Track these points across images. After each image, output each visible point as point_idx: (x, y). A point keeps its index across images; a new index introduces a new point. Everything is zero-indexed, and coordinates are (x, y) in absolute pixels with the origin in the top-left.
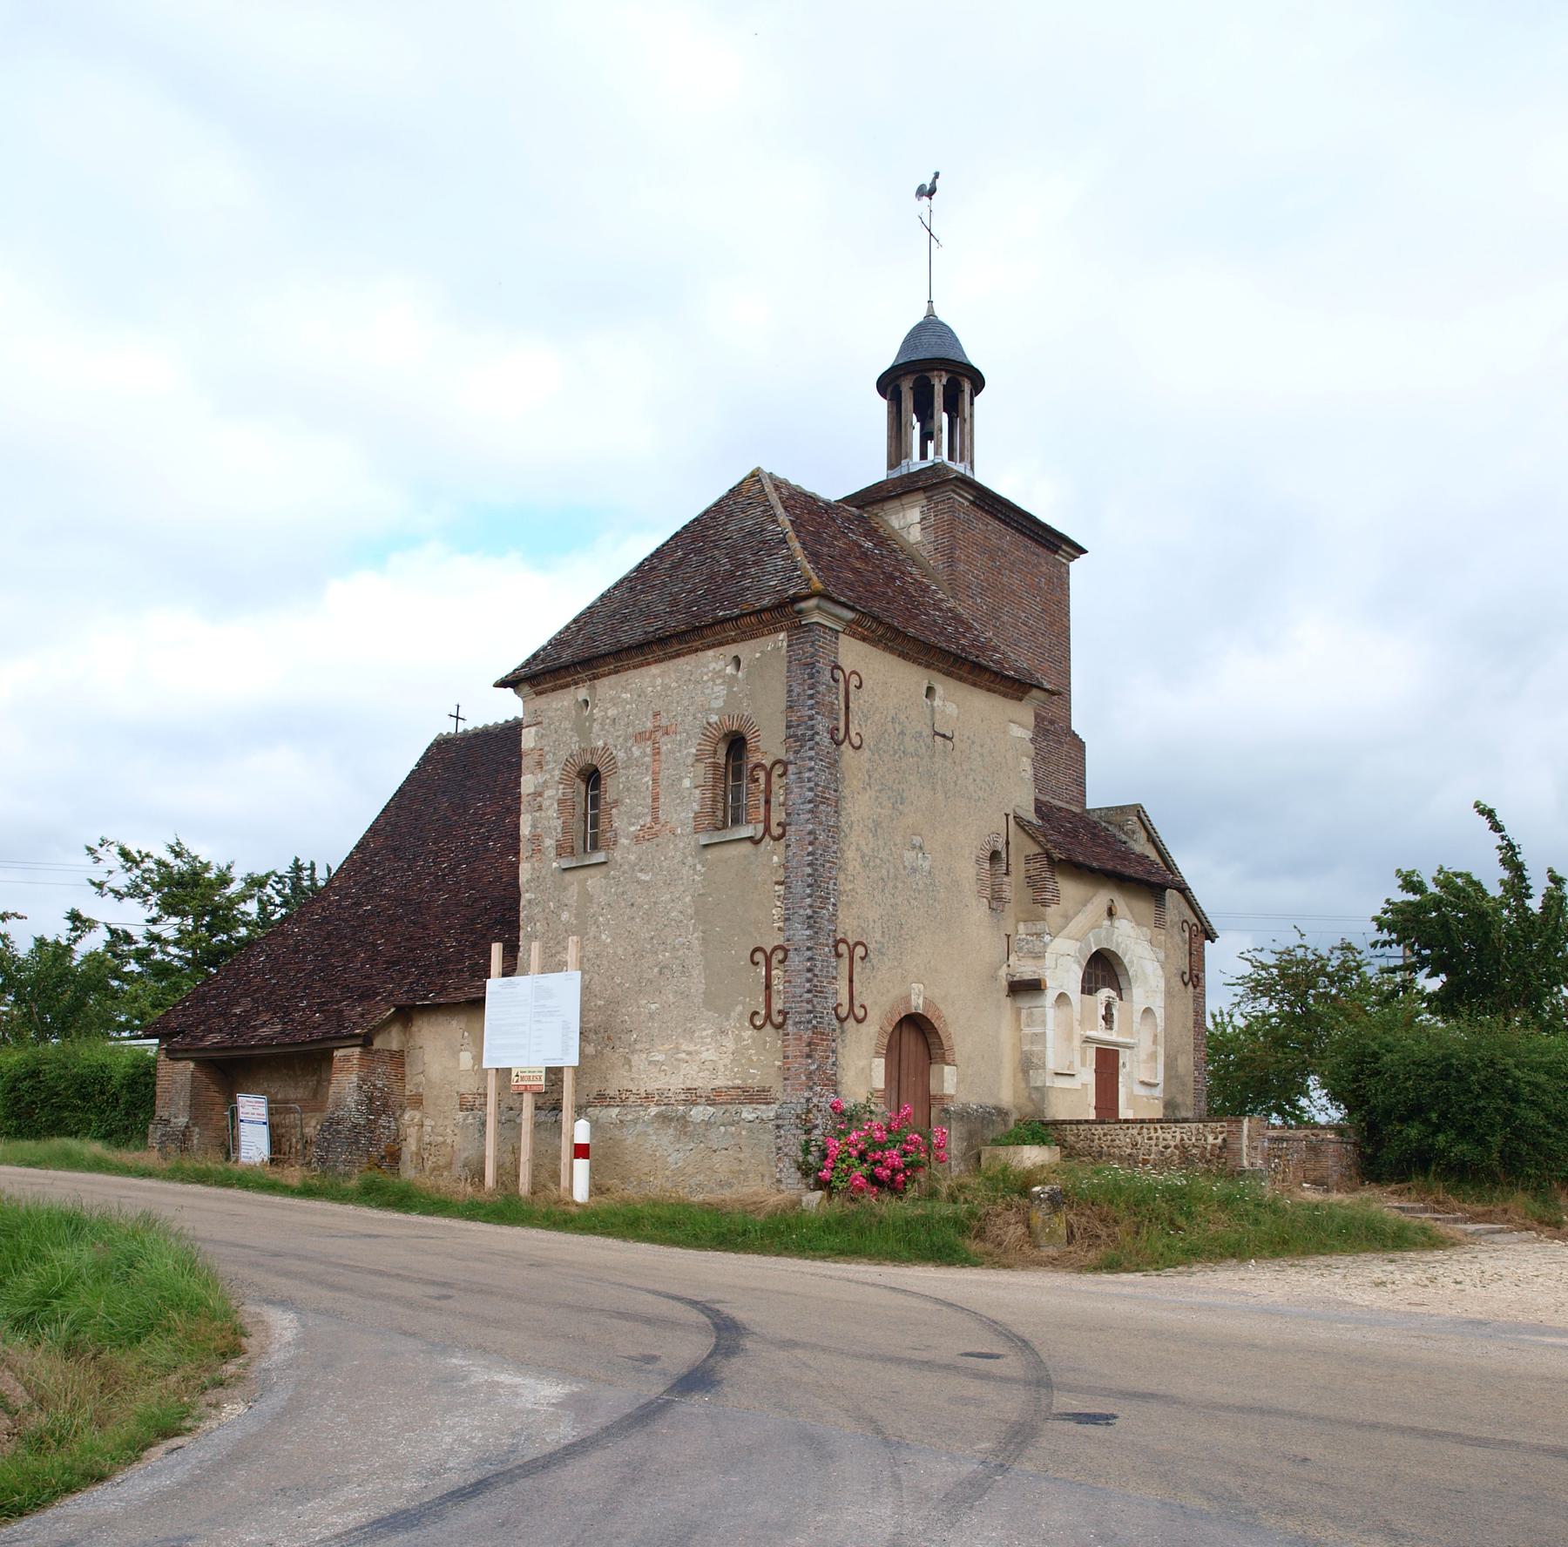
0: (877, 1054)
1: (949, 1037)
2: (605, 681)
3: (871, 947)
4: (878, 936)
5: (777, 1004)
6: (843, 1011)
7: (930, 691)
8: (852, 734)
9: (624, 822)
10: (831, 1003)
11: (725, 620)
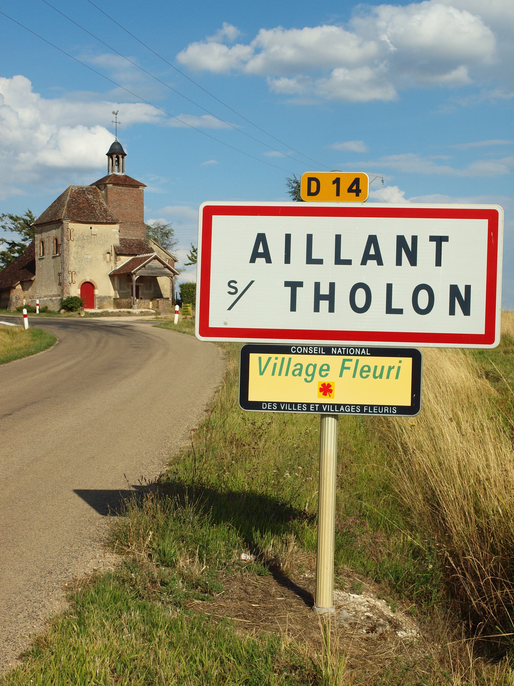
0: (79, 288)
1: (96, 285)
2: (43, 227)
3: (76, 272)
4: (78, 270)
5: (61, 282)
6: (71, 282)
7: (91, 228)
8: (72, 239)
9: (46, 252)
10: (68, 281)
11: (53, 221)
